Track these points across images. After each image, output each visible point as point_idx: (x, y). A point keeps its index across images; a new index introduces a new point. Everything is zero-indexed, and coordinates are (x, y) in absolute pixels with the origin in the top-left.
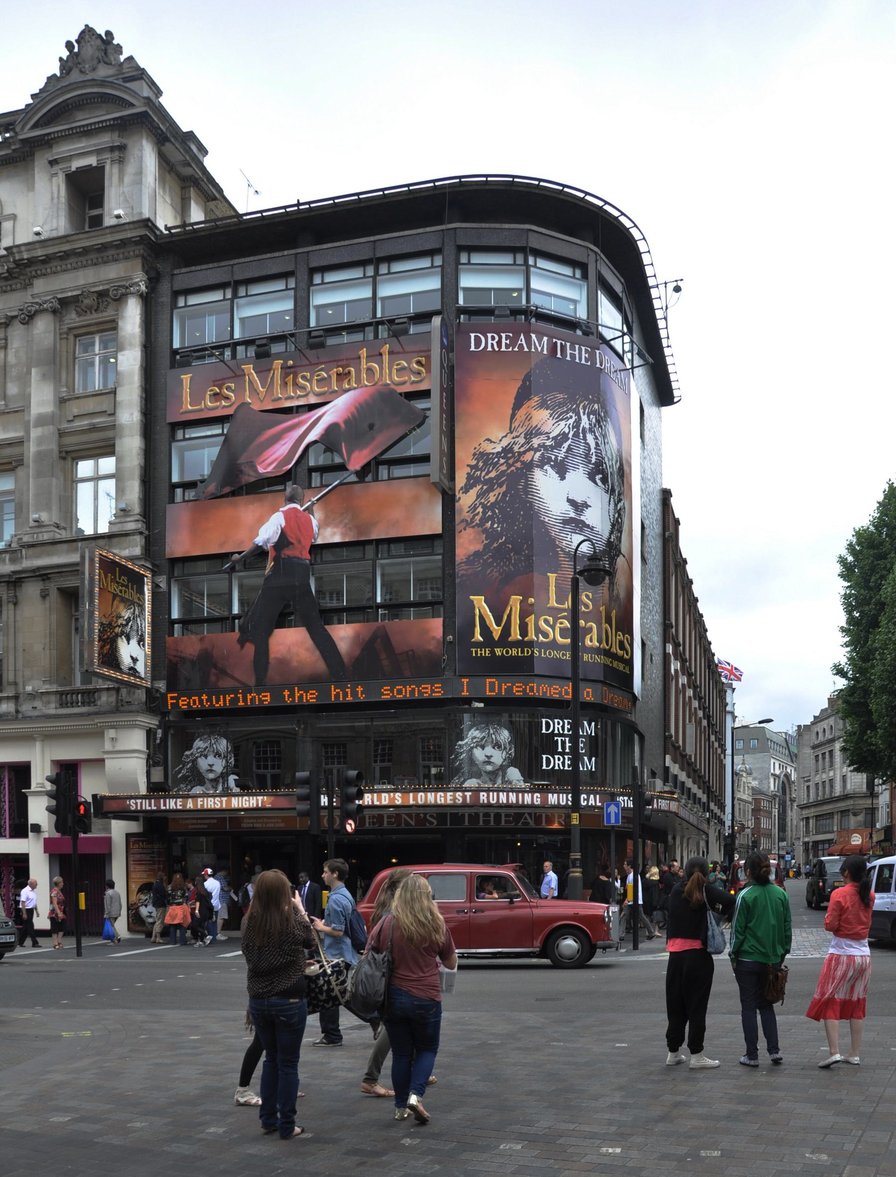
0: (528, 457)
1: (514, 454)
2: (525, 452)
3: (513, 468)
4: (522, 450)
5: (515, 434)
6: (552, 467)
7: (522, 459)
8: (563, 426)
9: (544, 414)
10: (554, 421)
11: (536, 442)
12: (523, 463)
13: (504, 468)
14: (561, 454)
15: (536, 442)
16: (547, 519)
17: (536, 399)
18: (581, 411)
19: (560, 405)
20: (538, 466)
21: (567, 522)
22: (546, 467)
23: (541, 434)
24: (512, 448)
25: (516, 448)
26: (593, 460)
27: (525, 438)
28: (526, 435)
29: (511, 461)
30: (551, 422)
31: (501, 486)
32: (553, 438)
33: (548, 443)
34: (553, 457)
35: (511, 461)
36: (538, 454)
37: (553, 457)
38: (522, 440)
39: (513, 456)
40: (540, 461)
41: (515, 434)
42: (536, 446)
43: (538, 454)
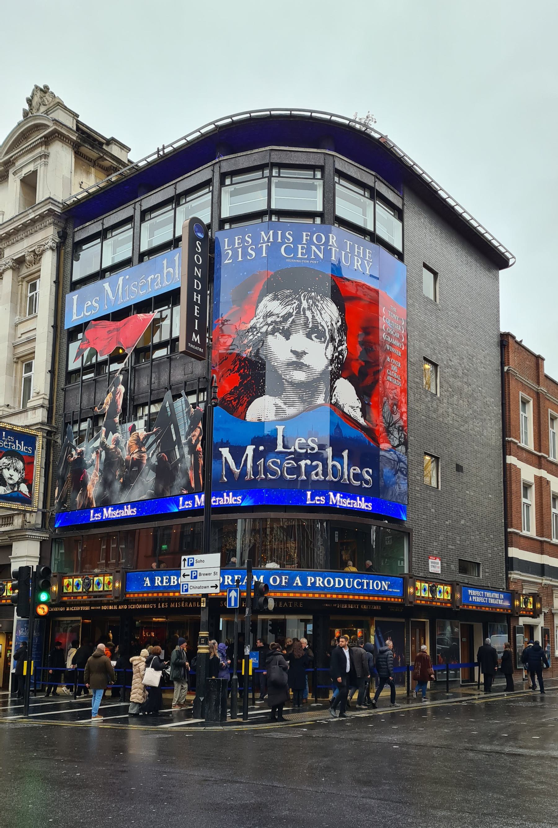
0: (264, 330)
1: (256, 328)
2: (262, 327)
3: (256, 337)
4: (262, 325)
5: (258, 317)
6: (280, 333)
7: (261, 331)
8: (289, 309)
9: (277, 303)
10: (283, 306)
11: (269, 320)
12: (261, 333)
13: (251, 337)
14: (287, 325)
15: (269, 320)
16: (276, 364)
17: (271, 295)
18: (302, 298)
19: (287, 297)
20: (270, 334)
21: (290, 364)
22: (275, 334)
23: (273, 315)
24: (256, 325)
25: (258, 326)
26: (310, 326)
27: (263, 318)
28: (263, 317)
29: (255, 333)
30: (281, 307)
31: (249, 347)
32: (281, 317)
33: (278, 320)
34: (281, 328)
35: (255, 333)
36: (271, 327)
37: (281, 328)
38: (261, 320)
39: (257, 330)
40: (272, 331)
41: (258, 317)
42: (269, 322)
43: (271, 327)
